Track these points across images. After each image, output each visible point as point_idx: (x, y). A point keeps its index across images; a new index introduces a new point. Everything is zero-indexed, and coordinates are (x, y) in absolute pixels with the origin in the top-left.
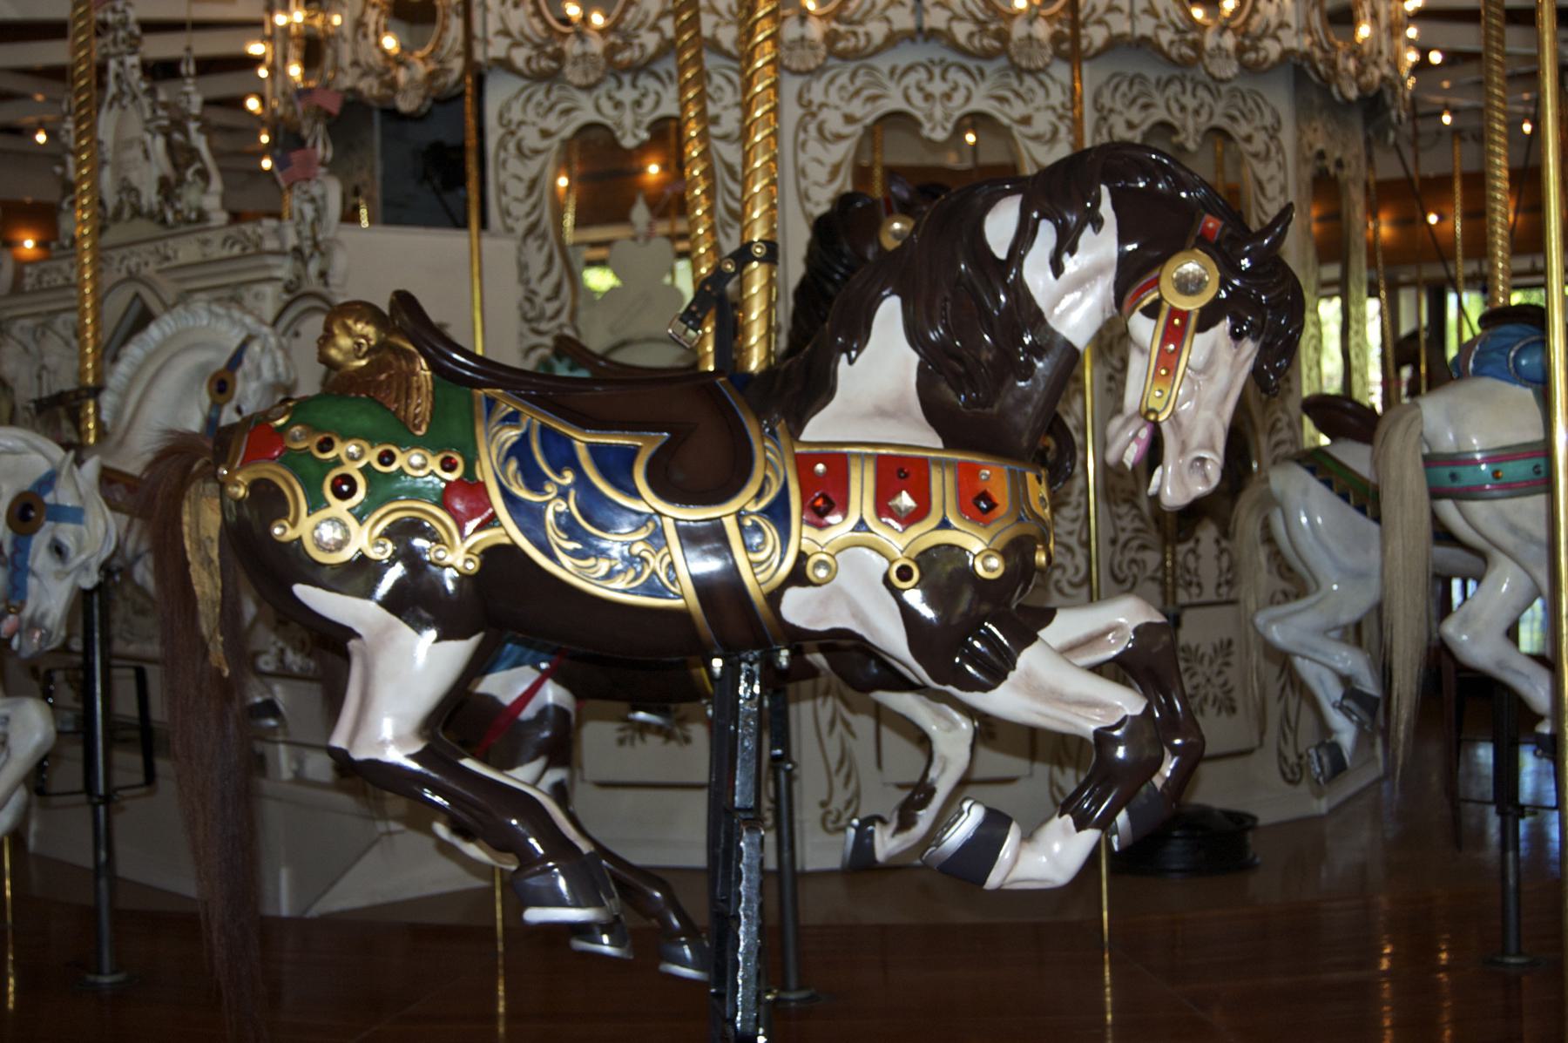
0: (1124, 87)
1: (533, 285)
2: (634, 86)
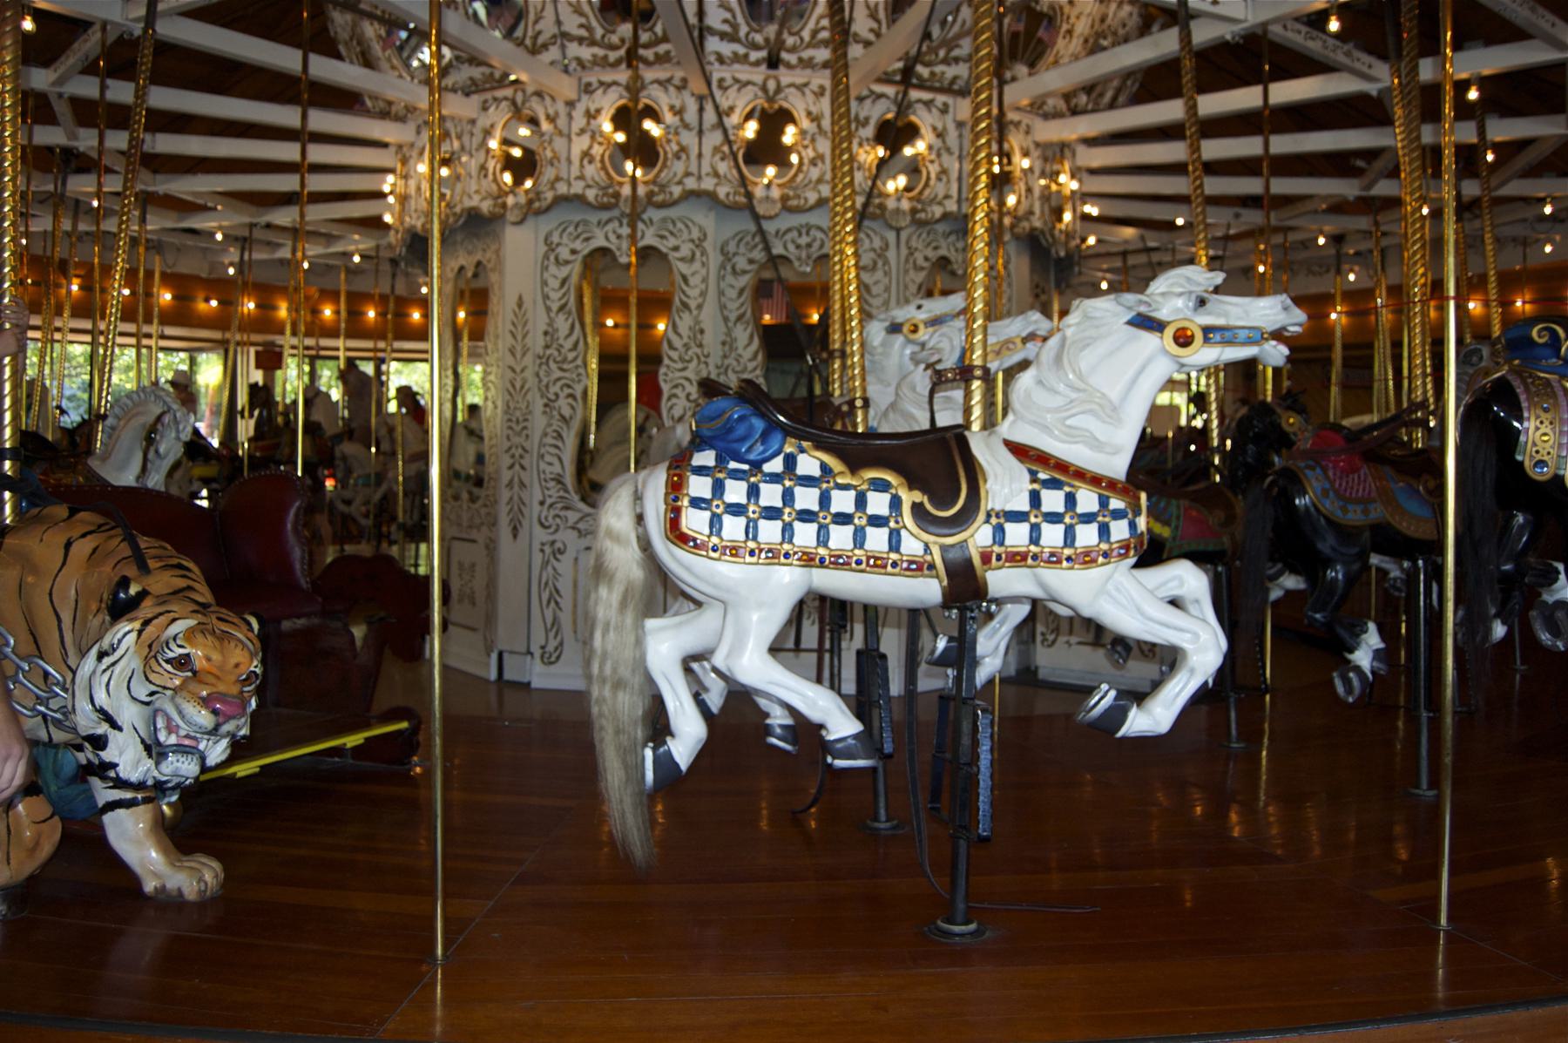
0: (571, 229)
1: (561, 341)
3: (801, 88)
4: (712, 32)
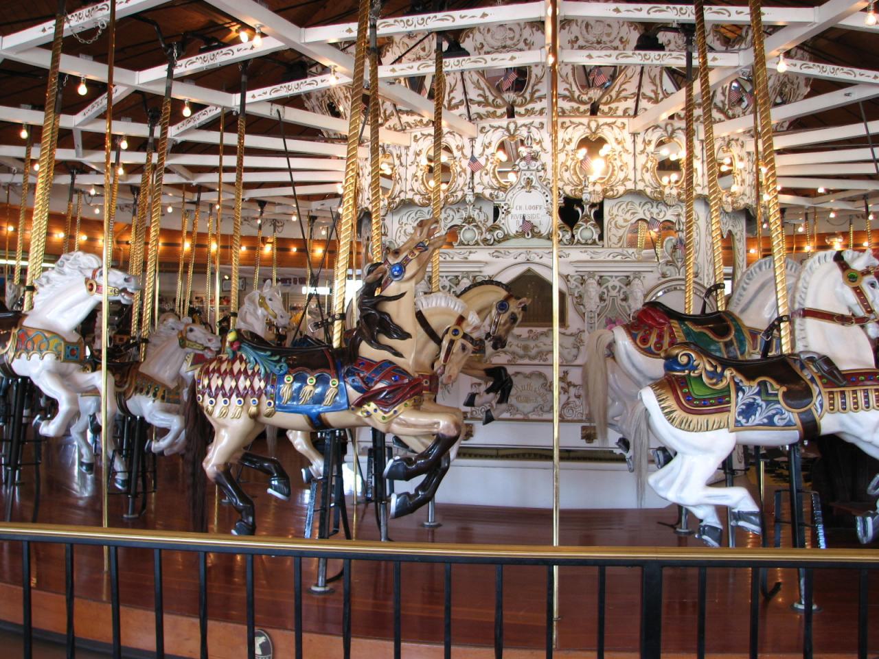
2: (657, 207)
3: (609, 125)
4: (645, 96)
